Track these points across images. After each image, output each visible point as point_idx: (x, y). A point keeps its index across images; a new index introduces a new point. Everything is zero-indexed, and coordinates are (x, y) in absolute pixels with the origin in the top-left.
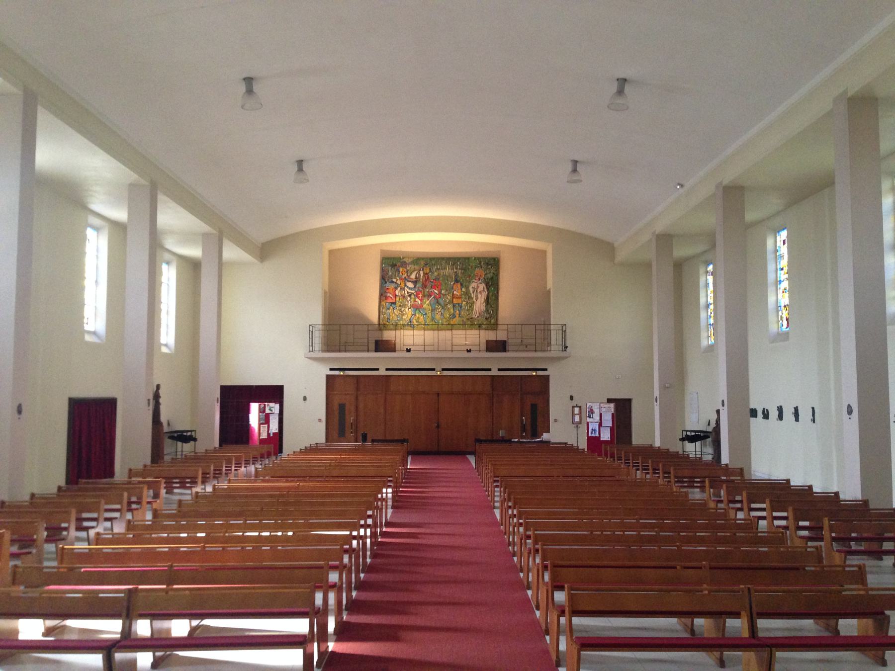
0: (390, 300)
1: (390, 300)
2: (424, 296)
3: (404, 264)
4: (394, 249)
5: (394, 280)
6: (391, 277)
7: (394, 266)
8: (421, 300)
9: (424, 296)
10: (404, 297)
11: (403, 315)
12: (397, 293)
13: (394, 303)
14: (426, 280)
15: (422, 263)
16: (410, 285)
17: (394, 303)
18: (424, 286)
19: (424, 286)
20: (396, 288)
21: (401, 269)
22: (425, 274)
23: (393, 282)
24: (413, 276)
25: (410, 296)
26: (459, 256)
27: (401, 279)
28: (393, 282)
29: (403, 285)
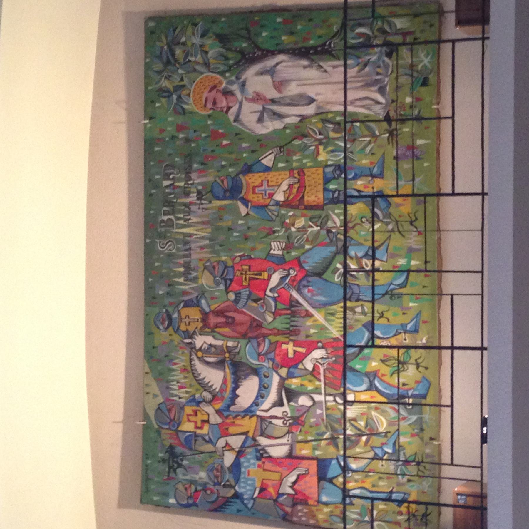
0: (310, 486)
1: (310, 486)
2: (291, 332)
3: (168, 414)
4: (115, 433)
5: (229, 459)
6: (217, 471)
7: (173, 459)
8: (311, 346)
9: (291, 332)
10: (296, 422)
11: (373, 433)
12: (279, 451)
13: (323, 464)
14: (230, 323)
15: (162, 336)
16: (248, 390)
17: (323, 464)
18: (254, 331)
19: (254, 331)
20: (262, 455)
21: (188, 427)
22: (206, 326)
23: (236, 466)
24: (215, 377)
25: (292, 395)
26: (141, 287)
27: (224, 431)
28: (236, 466)
29: (249, 424)
